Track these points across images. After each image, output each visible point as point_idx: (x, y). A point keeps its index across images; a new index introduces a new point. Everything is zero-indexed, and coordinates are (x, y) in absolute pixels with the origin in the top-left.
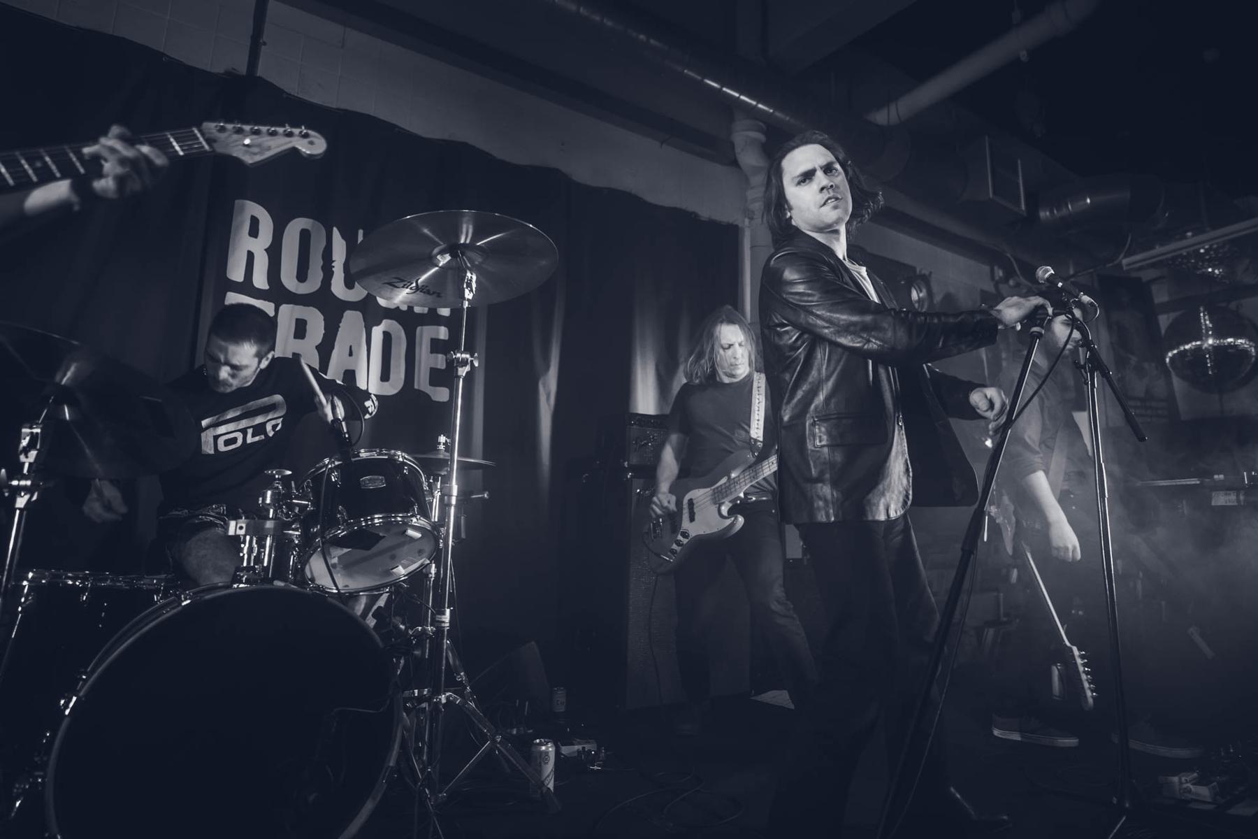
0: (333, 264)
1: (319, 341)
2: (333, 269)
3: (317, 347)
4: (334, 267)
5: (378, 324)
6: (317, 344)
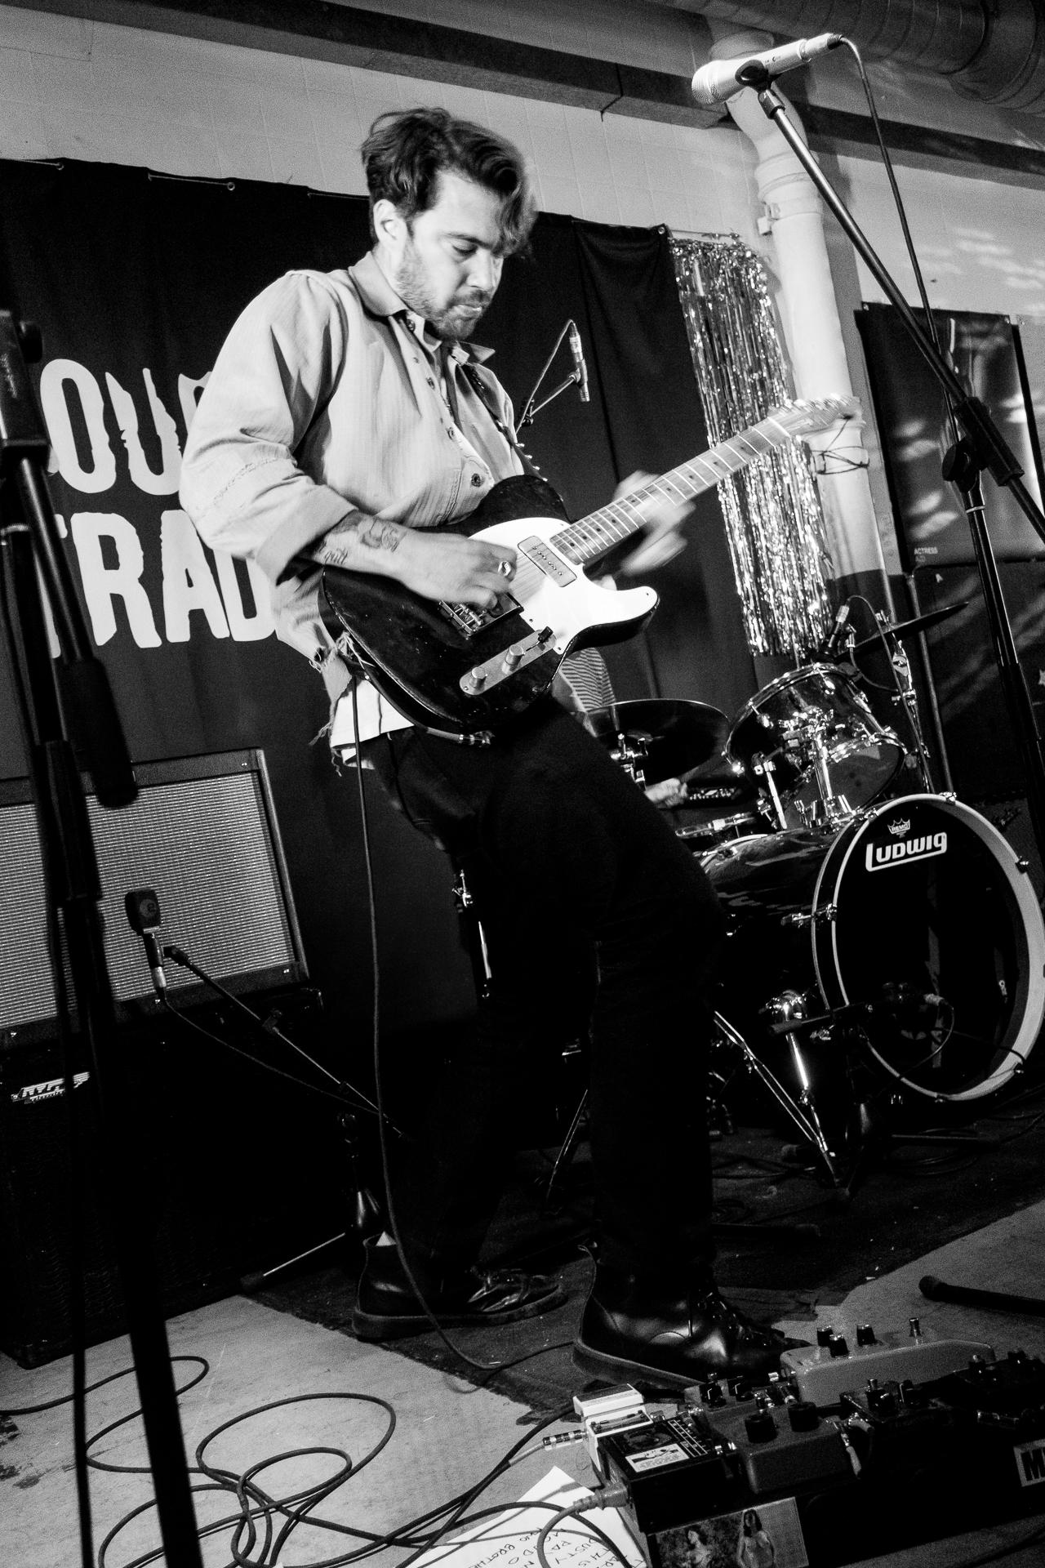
0: (123, 437)
1: (140, 570)
2: (126, 445)
3: (143, 580)
4: (125, 441)
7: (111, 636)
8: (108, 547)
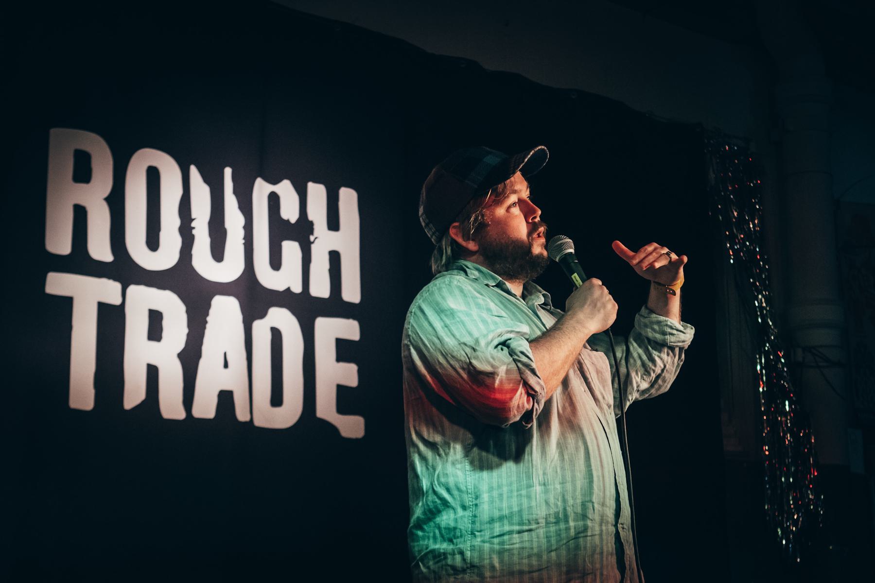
0: (193, 224)
2: (194, 232)
3: (180, 356)
4: (194, 228)
5: (262, 315)
8: (155, 319)
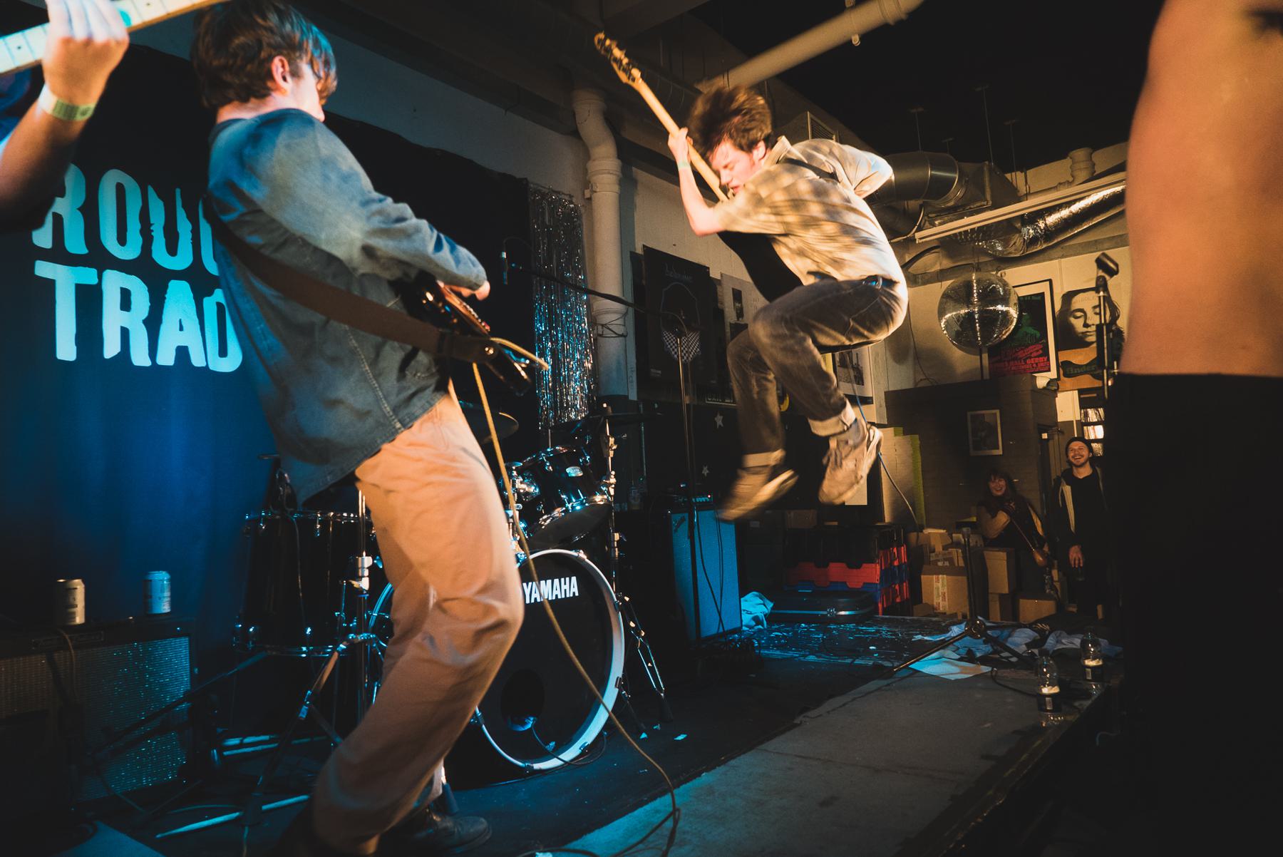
0: (152, 228)
1: (145, 314)
2: (153, 234)
3: (145, 322)
4: (152, 231)
5: (210, 294)
6: (144, 318)
7: (116, 353)
